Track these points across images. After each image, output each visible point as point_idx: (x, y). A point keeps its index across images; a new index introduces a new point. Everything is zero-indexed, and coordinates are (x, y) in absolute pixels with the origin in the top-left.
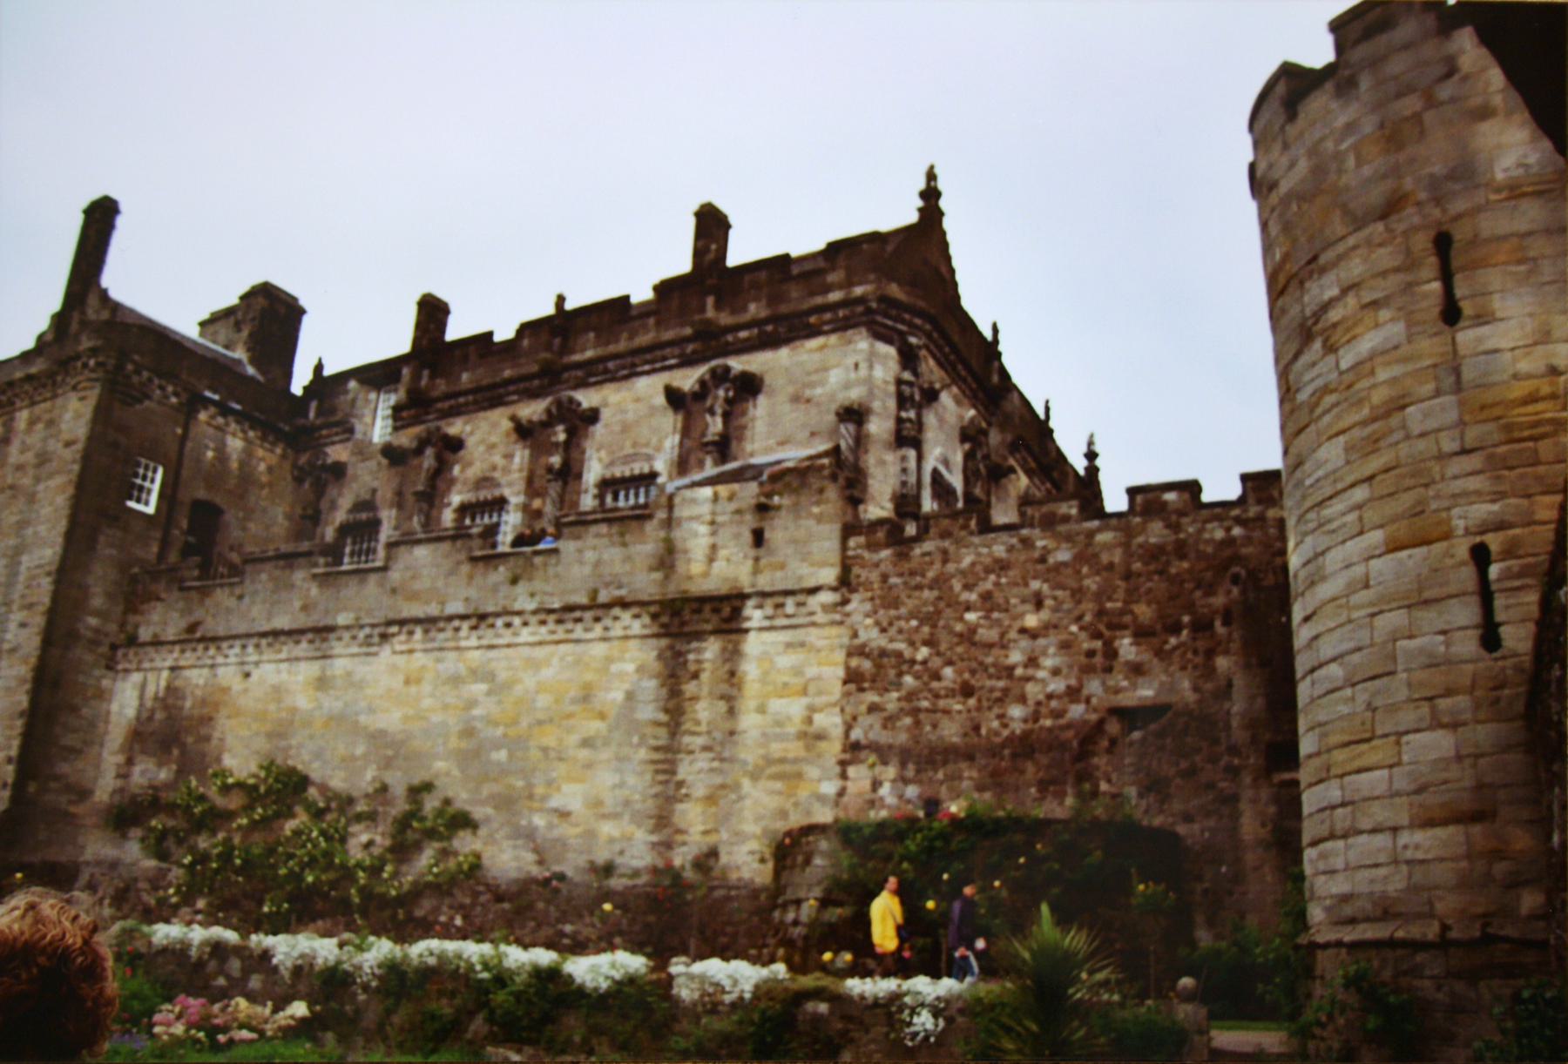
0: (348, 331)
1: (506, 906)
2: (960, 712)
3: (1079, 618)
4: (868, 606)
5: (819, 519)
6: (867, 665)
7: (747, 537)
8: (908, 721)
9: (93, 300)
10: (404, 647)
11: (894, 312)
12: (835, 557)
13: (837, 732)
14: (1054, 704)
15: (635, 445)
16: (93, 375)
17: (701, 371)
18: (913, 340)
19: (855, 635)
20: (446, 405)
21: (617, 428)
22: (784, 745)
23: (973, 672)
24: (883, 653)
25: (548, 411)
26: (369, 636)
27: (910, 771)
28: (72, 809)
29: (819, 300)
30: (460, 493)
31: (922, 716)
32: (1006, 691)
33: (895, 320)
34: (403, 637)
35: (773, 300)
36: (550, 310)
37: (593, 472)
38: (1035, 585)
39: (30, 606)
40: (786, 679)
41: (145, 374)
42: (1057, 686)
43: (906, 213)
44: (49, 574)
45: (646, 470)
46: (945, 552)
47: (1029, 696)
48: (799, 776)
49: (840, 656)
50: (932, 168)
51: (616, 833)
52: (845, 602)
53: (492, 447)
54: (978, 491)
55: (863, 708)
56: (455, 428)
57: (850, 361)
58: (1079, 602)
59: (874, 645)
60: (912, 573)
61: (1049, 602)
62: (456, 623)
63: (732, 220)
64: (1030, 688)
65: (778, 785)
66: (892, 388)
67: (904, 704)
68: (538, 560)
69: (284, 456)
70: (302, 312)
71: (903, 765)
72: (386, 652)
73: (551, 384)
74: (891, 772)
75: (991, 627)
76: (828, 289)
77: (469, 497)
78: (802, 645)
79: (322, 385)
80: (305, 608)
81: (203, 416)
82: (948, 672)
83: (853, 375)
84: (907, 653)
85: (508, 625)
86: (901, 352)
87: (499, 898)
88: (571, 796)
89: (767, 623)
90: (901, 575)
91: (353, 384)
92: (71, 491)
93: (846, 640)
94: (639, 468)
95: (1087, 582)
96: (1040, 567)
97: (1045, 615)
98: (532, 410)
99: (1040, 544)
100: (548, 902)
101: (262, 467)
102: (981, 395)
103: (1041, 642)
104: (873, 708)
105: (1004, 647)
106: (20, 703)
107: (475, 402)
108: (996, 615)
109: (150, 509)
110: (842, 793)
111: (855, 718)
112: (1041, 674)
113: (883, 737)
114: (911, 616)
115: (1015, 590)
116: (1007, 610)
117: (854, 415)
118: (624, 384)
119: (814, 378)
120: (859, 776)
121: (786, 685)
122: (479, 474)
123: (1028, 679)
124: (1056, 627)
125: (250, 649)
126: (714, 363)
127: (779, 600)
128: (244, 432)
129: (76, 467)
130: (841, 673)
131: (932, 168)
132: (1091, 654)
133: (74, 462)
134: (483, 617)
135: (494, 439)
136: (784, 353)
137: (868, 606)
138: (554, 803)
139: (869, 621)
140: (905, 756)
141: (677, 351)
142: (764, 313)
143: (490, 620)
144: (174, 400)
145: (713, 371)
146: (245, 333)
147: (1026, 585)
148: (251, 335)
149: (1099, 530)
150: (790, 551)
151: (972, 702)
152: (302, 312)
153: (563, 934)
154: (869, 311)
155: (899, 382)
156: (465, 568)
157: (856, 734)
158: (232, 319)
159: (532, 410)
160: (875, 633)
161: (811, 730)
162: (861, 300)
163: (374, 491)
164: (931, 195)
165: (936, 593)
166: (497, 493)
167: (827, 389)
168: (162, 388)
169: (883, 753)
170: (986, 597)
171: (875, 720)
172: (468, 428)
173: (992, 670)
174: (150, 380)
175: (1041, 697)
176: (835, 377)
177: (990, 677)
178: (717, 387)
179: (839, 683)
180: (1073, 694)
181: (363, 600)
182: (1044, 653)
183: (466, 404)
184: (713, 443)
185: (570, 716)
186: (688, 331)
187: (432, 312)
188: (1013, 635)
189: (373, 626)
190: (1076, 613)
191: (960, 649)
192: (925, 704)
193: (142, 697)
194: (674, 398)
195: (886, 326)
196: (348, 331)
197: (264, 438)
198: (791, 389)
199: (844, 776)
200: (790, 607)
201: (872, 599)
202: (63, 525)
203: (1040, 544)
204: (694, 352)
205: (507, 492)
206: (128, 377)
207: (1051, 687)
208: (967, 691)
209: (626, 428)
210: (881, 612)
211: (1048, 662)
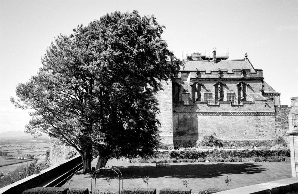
6: (277, 119)
7: (264, 106)
20: (200, 79)
24: (279, 118)
71: (282, 128)
82: (286, 120)
87: (242, 142)
107: (205, 80)
110: (276, 131)
126: (241, 81)
133: (170, 88)
145: (241, 82)
156: (231, 106)
157: (277, 126)
163: (188, 89)
193: (178, 119)
199: (276, 129)
205: (212, 93)
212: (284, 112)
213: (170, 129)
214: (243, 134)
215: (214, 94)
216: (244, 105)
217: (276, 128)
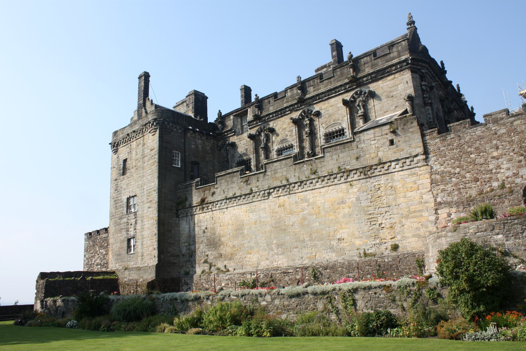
0: (222, 103)
1: (328, 271)
2: (475, 187)
3: (514, 150)
4: (435, 158)
5: (412, 132)
6: (438, 177)
7: (388, 143)
8: (456, 193)
9: (148, 104)
10: (277, 195)
11: (416, 63)
12: (421, 144)
13: (433, 200)
14: (509, 179)
15: (334, 120)
16: (156, 127)
17: (351, 93)
18: (423, 71)
19: (432, 168)
21: (327, 116)
22: (414, 207)
23: (477, 174)
24: (443, 172)
25: (301, 115)
26: (264, 194)
27: (461, 209)
28: (174, 261)
29: (390, 63)
30: (277, 145)
31: (461, 190)
32: (490, 178)
33: (417, 66)
34: (275, 192)
35: (373, 66)
36: (295, 82)
37: (321, 132)
38: (494, 142)
39: (151, 201)
40: (410, 186)
41: (171, 124)
42: (509, 173)
43: (404, 31)
44: (154, 191)
45: (340, 128)
46: (459, 136)
47: (499, 178)
48: (421, 216)
49: (428, 176)
50: (410, 14)
51: (361, 243)
52: (427, 158)
53: (285, 129)
54: (446, 118)
55: (440, 191)
56: (271, 125)
57: (405, 81)
58: (512, 145)
59: (439, 170)
60: (449, 145)
61: (500, 147)
62: (293, 185)
63: (342, 44)
64: (499, 175)
65: (415, 220)
66: (420, 88)
67: (454, 188)
68: (316, 161)
69: (214, 143)
70: (207, 98)
71: (458, 207)
72: (271, 197)
73: (301, 106)
74: (454, 210)
75: (481, 158)
76: (393, 59)
77: (280, 146)
78: (414, 174)
79: (222, 118)
80: (240, 188)
81: (189, 135)
82: (468, 175)
83: (406, 86)
84: (452, 171)
85: (312, 183)
86: (420, 75)
88: (343, 233)
89: (401, 169)
90: (445, 146)
91: (232, 117)
92: (157, 164)
93: (430, 171)
94: (338, 127)
95: (513, 138)
96: (494, 136)
97: (500, 151)
98: (296, 115)
99: (493, 129)
100: (342, 267)
101: (208, 148)
102: (442, 86)
103: (500, 160)
104: (443, 190)
105: (486, 164)
106: (154, 231)
107: (276, 116)
108: (481, 154)
109: (179, 166)
110: (437, 219)
111: (437, 195)
112: (502, 171)
113: (449, 199)
114: (451, 159)
115: (487, 145)
116: (486, 152)
117: (410, 98)
118: (326, 102)
119: (393, 88)
120: (443, 213)
121: (411, 187)
122: (282, 139)
123: (498, 173)
124: (505, 155)
125: (223, 204)
127: (404, 161)
128: (201, 138)
129: (157, 156)
130: (429, 180)
131: (410, 14)
132: (520, 161)
134: (301, 182)
135: (284, 126)
136: (380, 82)
137: (435, 158)
138: (338, 236)
139: (436, 163)
140: (458, 204)
141: (343, 88)
142: (371, 71)
143: (305, 183)
144: (180, 131)
145: (356, 93)
146: (191, 107)
147: (491, 142)
148: (193, 107)
149: (515, 121)
150: (404, 145)
151: (478, 183)
152: (207, 98)
153: (349, 277)
154: (408, 64)
155: (421, 85)
157: (439, 200)
158: (185, 104)
159: (296, 115)
160: (438, 166)
161: (423, 201)
162: (406, 60)
163: (247, 150)
164: (411, 23)
165: (458, 150)
166: (290, 144)
167: (398, 91)
168: (176, 128)
169: (449, 204)
170: (477, 149)
171: (445, 194)
172: (275, 124)
173: (484, 172)
174: (172, 126)
175: (504, 178)
176: (401, 87)
177: (484, 174)
178: (359, 97)
179: (429, 184)
180: (516, 175)
181: (259, 183)
182: (502, 164)
183: (273, 117)
184: (362, 116)
185: (338, 208)
186: (347, 81)
187: (247, 91)
188: (489, 159)
189: (266, 190)
190: (511, 149)
191: (471, 167)
192: (461, 186)
194: (345, 102)
195: (414, 68)
196: (222, 103)
197: (207, 139)
198: (385, 94)
200: (408, 163)
201: (436, 155)
202: (156, 175)
203: (493, 129)
204: (349, 87)
206: (166, 126)
207: (507, 175)
208: (477, 180)
209: (330, 116)
210: (440, 159)
211: (505, 166)
212: (460, 146)
213: (155, 249)
214: (332, 242)
215: (295, 145)
216: (327, 155)
217: (436, 210)
